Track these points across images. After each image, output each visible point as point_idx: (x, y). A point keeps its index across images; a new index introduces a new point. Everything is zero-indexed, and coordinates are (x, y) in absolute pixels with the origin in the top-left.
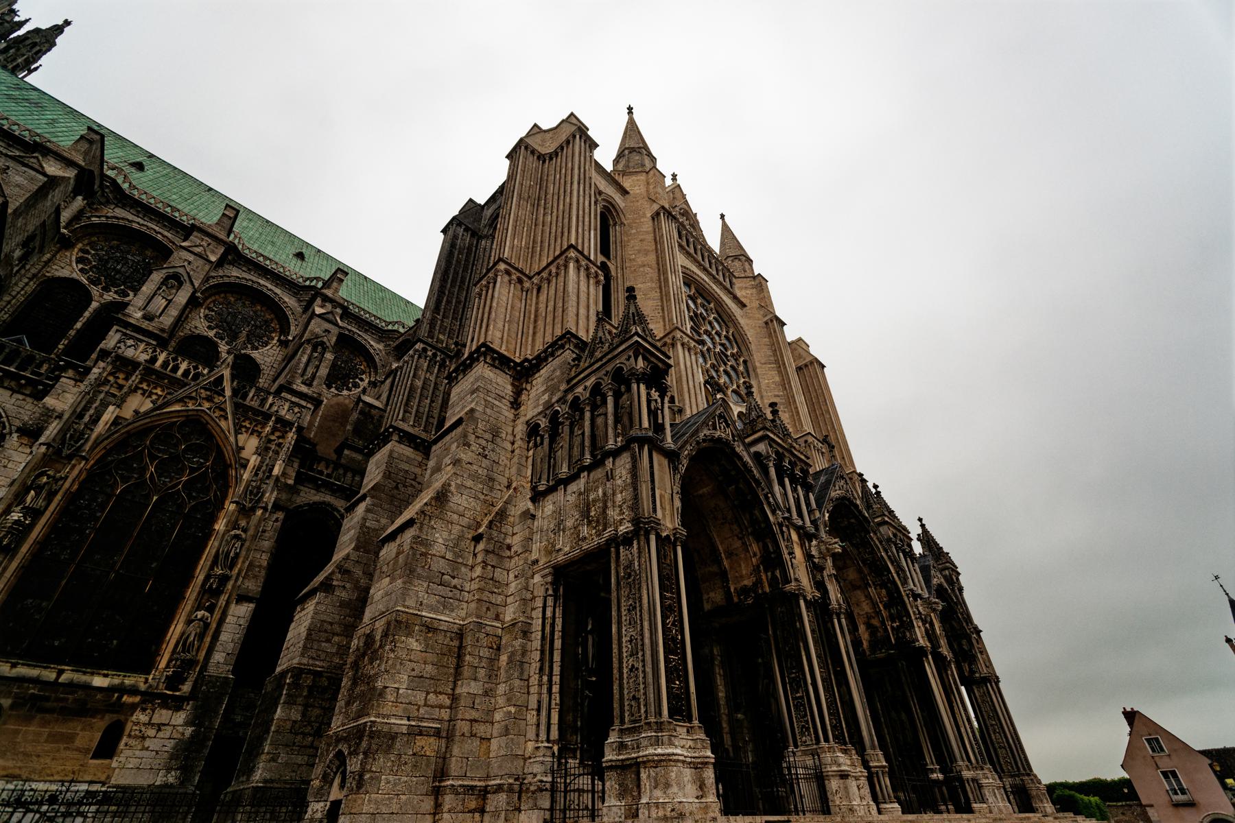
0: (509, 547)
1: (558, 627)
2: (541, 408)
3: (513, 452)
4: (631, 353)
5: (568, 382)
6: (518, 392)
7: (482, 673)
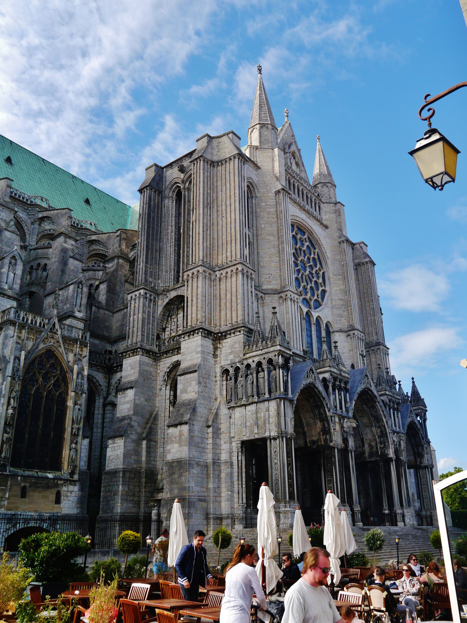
2: (229, 362)
3: (216, 381)
4: (277, 354)
5: (244, 355)
6: (216, 349)
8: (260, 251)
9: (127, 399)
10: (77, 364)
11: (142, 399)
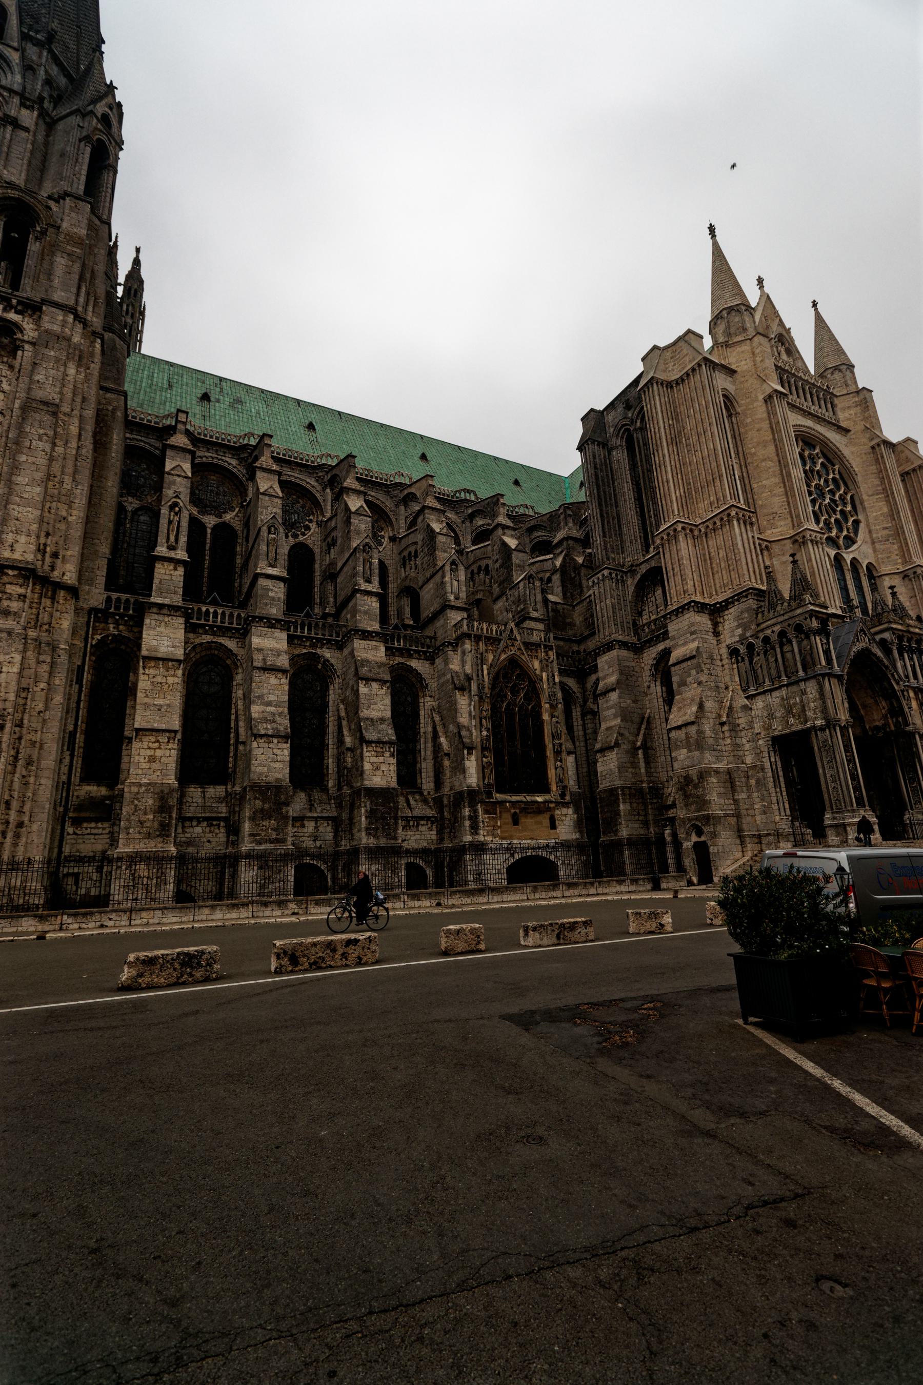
0: (738, 725)
1: (779, 765)
2: (737, 639)
3: (723, 666)
5: (758, 625)
6: (715, 625)
7: (745, 789)
8: (755, 486)
9: (611, 703)
10: (544, 670)
11: (628, 701)
